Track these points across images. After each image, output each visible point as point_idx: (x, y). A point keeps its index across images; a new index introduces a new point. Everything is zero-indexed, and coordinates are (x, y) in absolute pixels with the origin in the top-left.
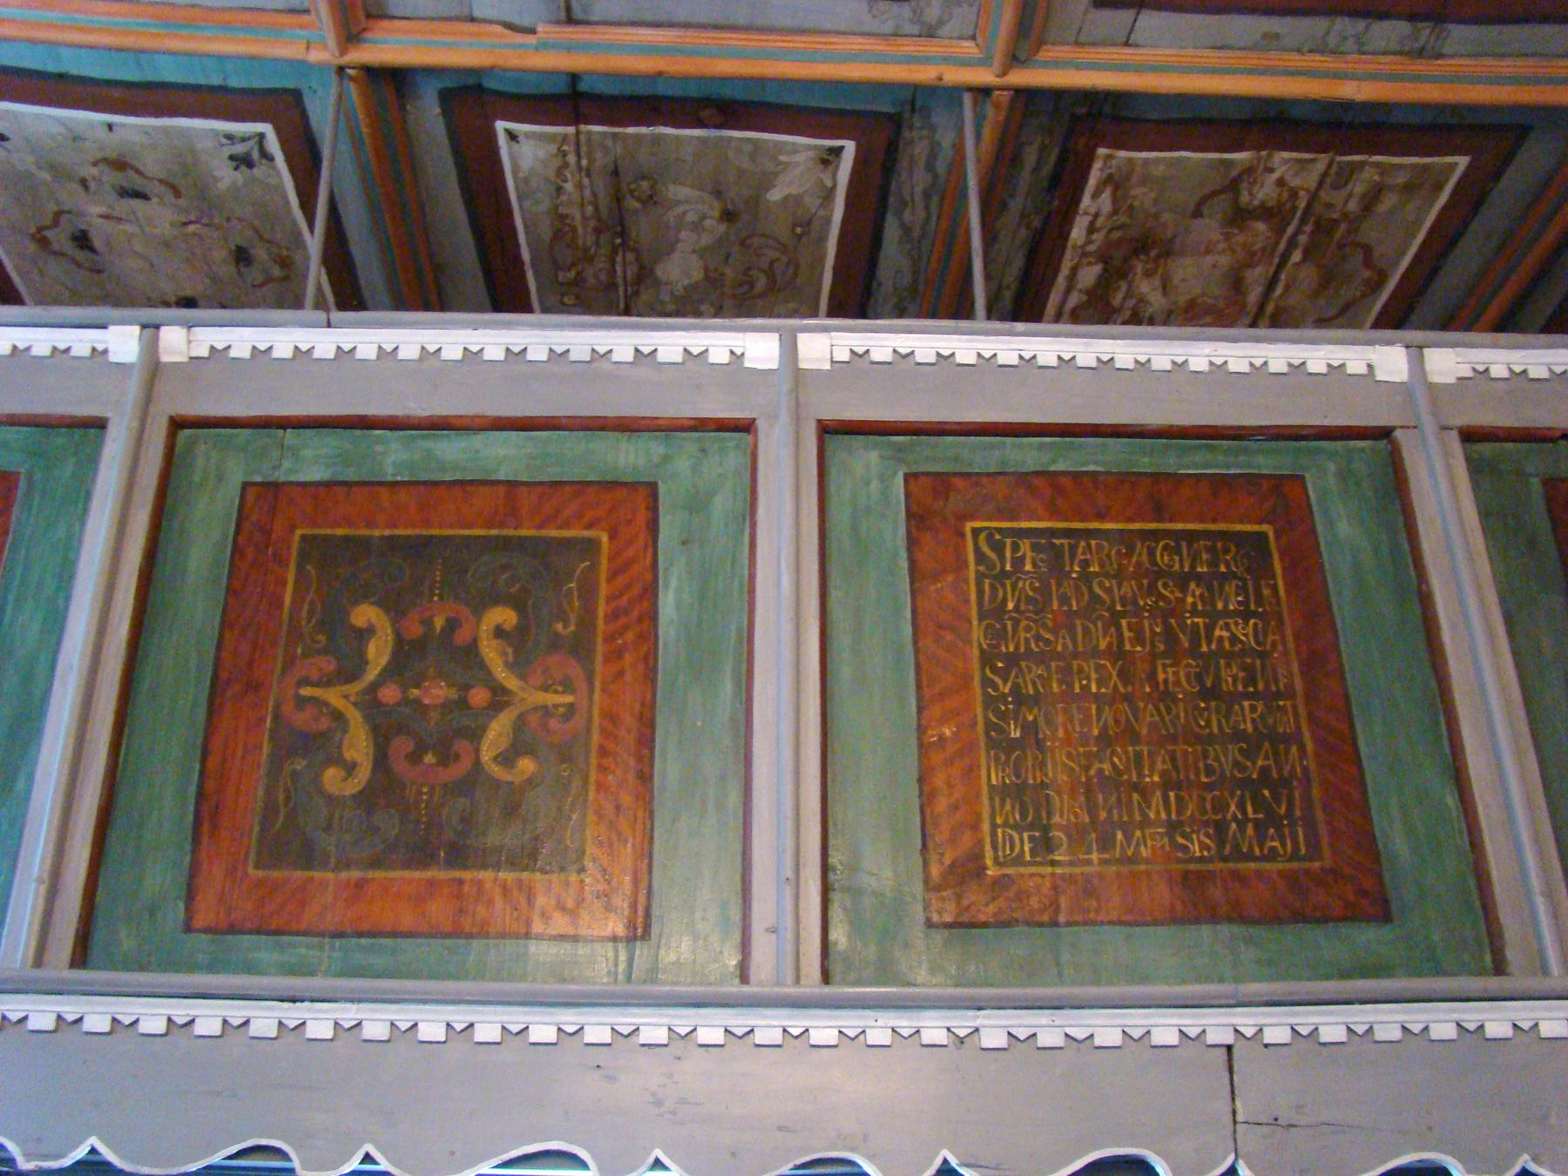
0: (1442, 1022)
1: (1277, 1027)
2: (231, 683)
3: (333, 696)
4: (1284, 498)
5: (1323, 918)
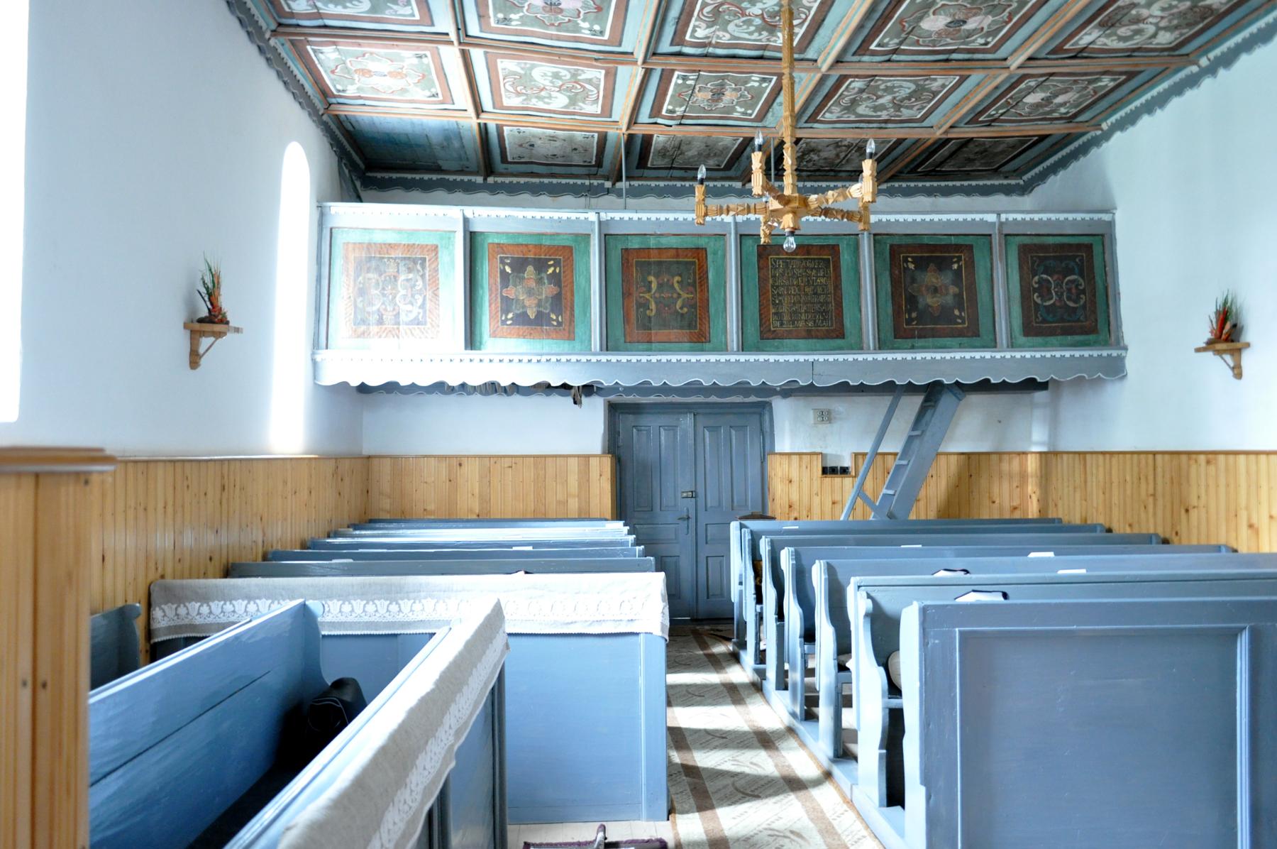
0: (850, 358)
1: (821, 358)
2: (626, 294)
3: (647, 296)
4: (834, 249)
5: (832, 338)
